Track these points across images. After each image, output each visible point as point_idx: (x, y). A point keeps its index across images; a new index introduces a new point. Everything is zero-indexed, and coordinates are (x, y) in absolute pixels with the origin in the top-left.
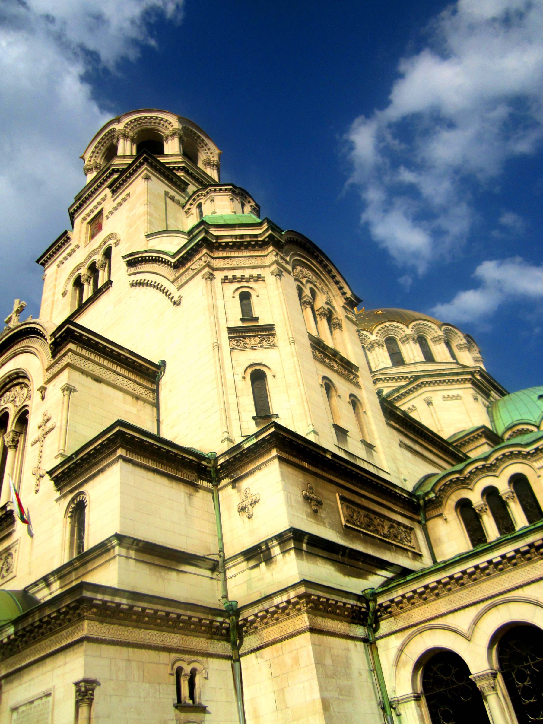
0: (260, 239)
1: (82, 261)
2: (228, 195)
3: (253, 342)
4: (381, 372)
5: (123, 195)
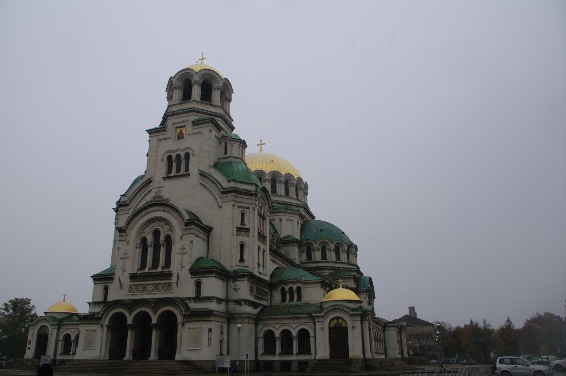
0: (251, 192)
2: (238, 144)
3: (243, 233)
4: (287, 324)
5: (198, 130)
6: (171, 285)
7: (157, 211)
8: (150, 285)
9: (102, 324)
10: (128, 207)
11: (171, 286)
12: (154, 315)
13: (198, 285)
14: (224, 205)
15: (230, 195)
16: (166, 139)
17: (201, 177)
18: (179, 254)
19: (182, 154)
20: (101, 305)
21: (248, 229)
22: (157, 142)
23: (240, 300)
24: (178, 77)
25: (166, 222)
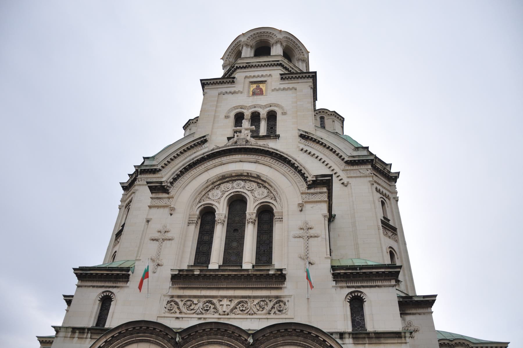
0: (390, 175)
1: (248, 105)
3: (390, 234)
5: (291, 86)
6: (282, 301)
7: (241, 161)
8: (225, 299)
11: (281, 304)
14: (352, 181)
15: (363, 167)
16: (234, 93)
17: (304, 141)
18: (300, 237)
19: (263, 113)
20: (89, 335)
22: (218, 96)
24: (251, 36)
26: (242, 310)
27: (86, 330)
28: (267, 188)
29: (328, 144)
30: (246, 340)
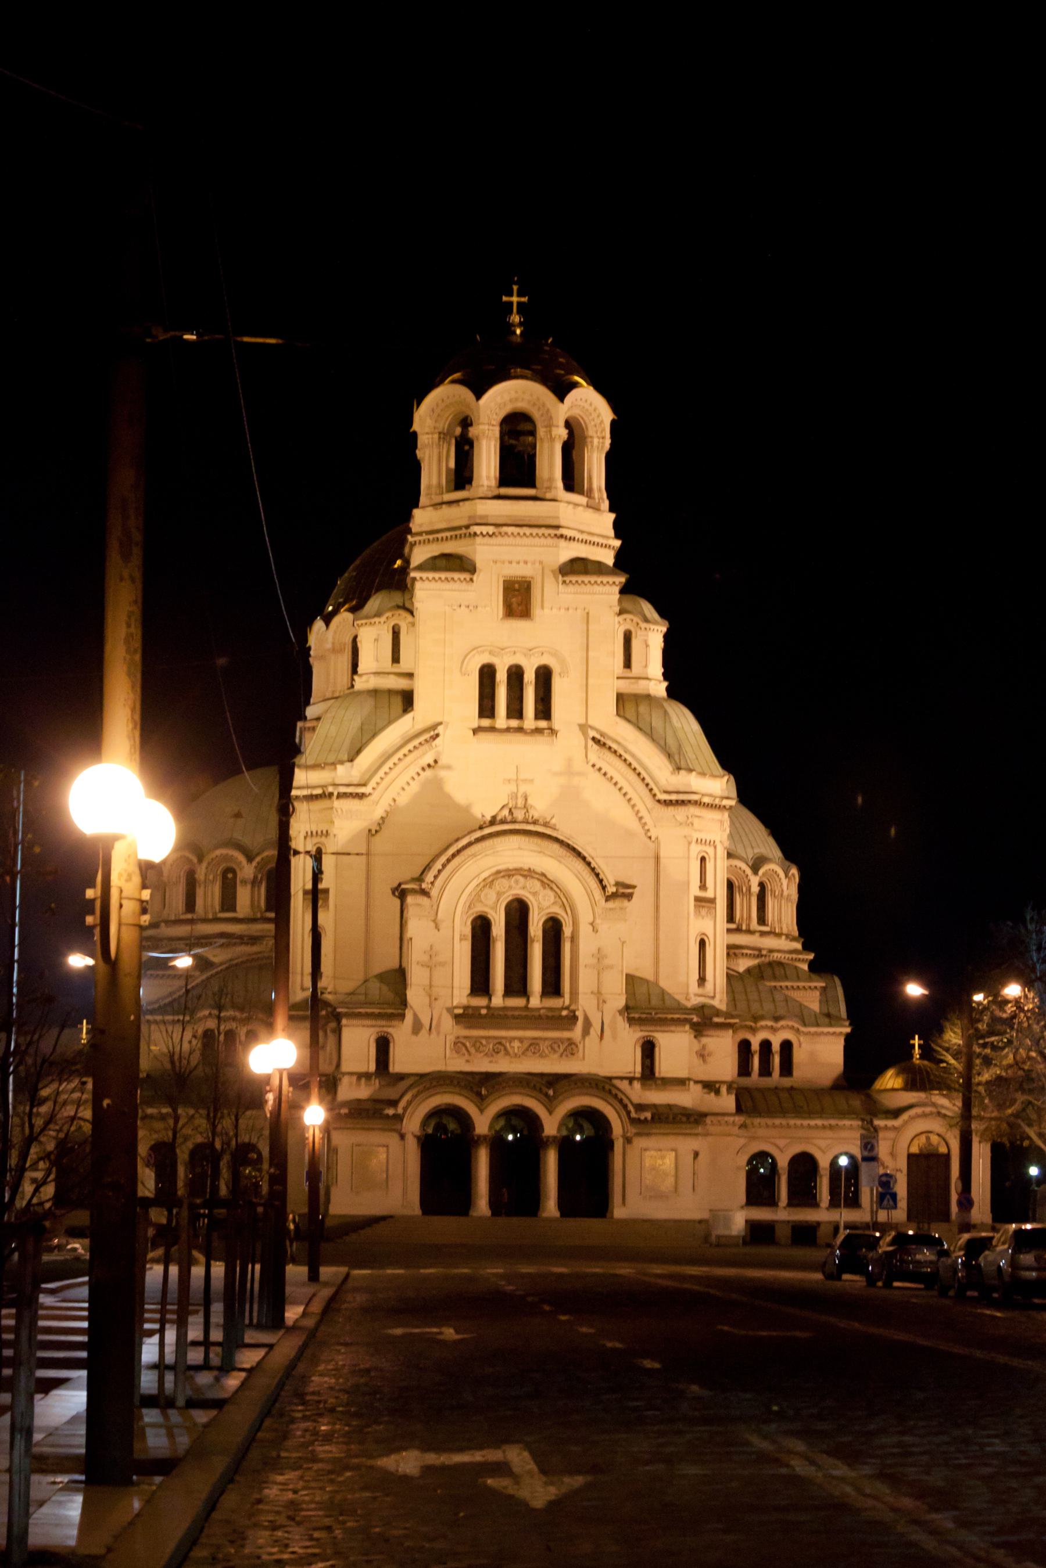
3: (704, 912)
6: (574, 1044)
9: (403, 1131)
10: (366, 801)
11: (573, 1046)
12: (547, 1113)
13: (649, 1049)
17: (596, 747)
20: (377, 1081)
21: (712, 901)
23: (716, 1082)
25: (545, 880)
26: (534, 1053)
27: (374, 1077)
28: (555, 891)
29: (635, 764)
30: (547, 1093)
